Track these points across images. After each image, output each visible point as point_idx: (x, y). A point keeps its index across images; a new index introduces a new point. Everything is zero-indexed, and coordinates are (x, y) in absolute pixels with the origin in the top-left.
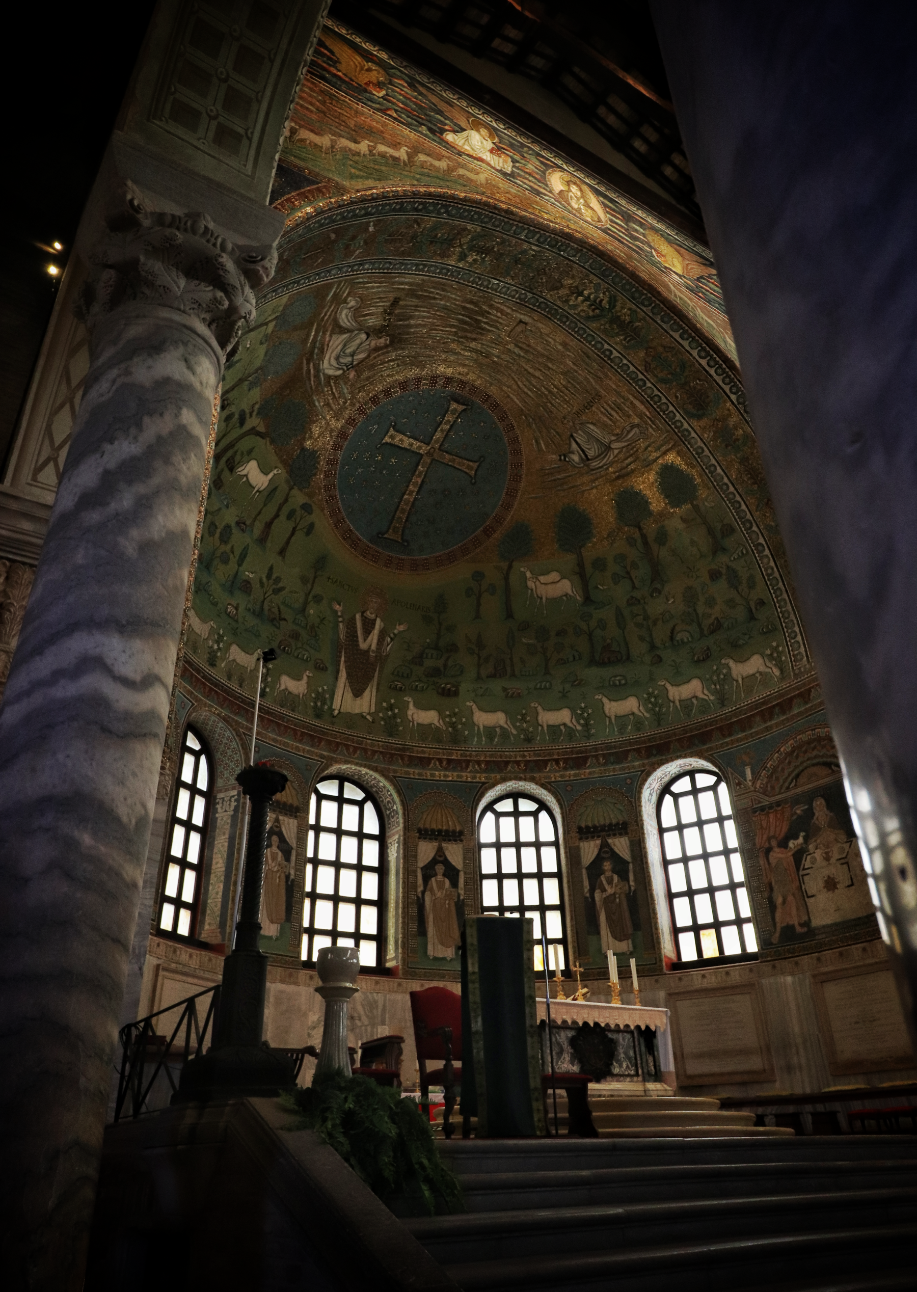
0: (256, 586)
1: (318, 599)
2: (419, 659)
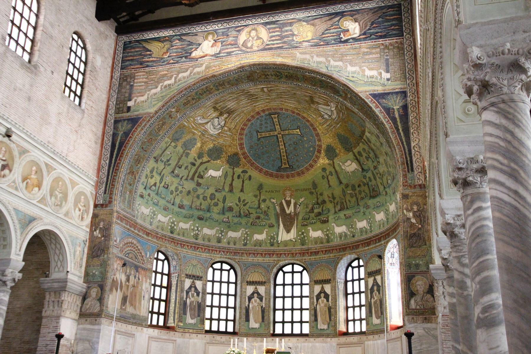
0: (235, 207)
1: (264, 201)
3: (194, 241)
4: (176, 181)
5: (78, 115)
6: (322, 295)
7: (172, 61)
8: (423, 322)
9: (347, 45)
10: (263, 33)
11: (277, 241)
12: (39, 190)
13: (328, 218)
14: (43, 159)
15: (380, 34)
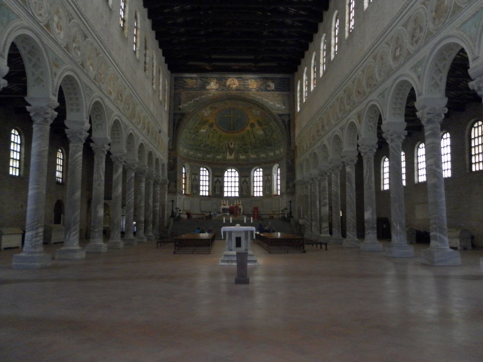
1: (221, 142)
2: (241, 147)
6: (245, 182)
7: (197, 89)
10: (236, 82)
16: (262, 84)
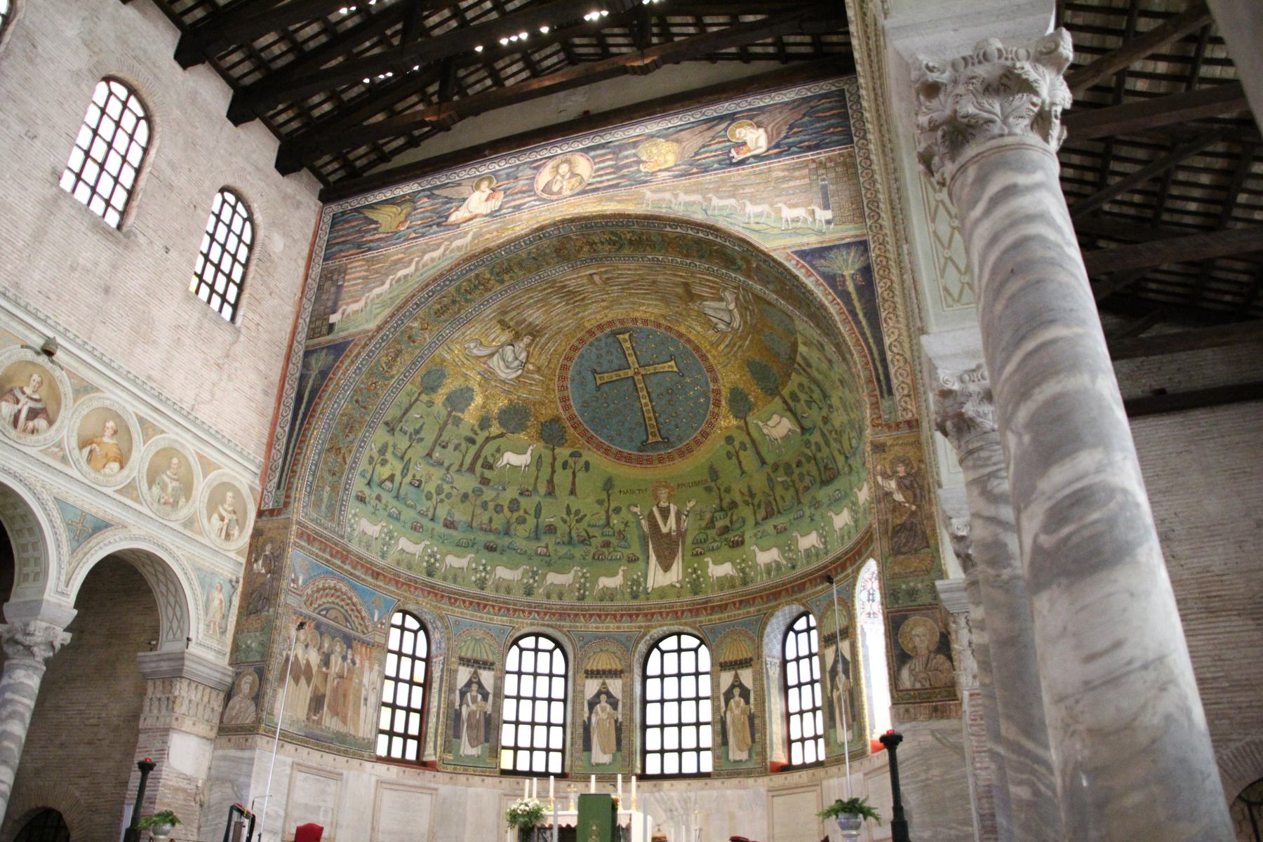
1: (617, 510)
3: (478, 591)
4: (437, 474)
5: (224, 336)
6: (737, 691)
8: (930, 718)
9: (743, 169)
10: (584, 166)
11: (646, 589)
12: (122, 467)
13: (742, 536)
14: (131, 408)
15: (806, 143)
16: (704, 146)
